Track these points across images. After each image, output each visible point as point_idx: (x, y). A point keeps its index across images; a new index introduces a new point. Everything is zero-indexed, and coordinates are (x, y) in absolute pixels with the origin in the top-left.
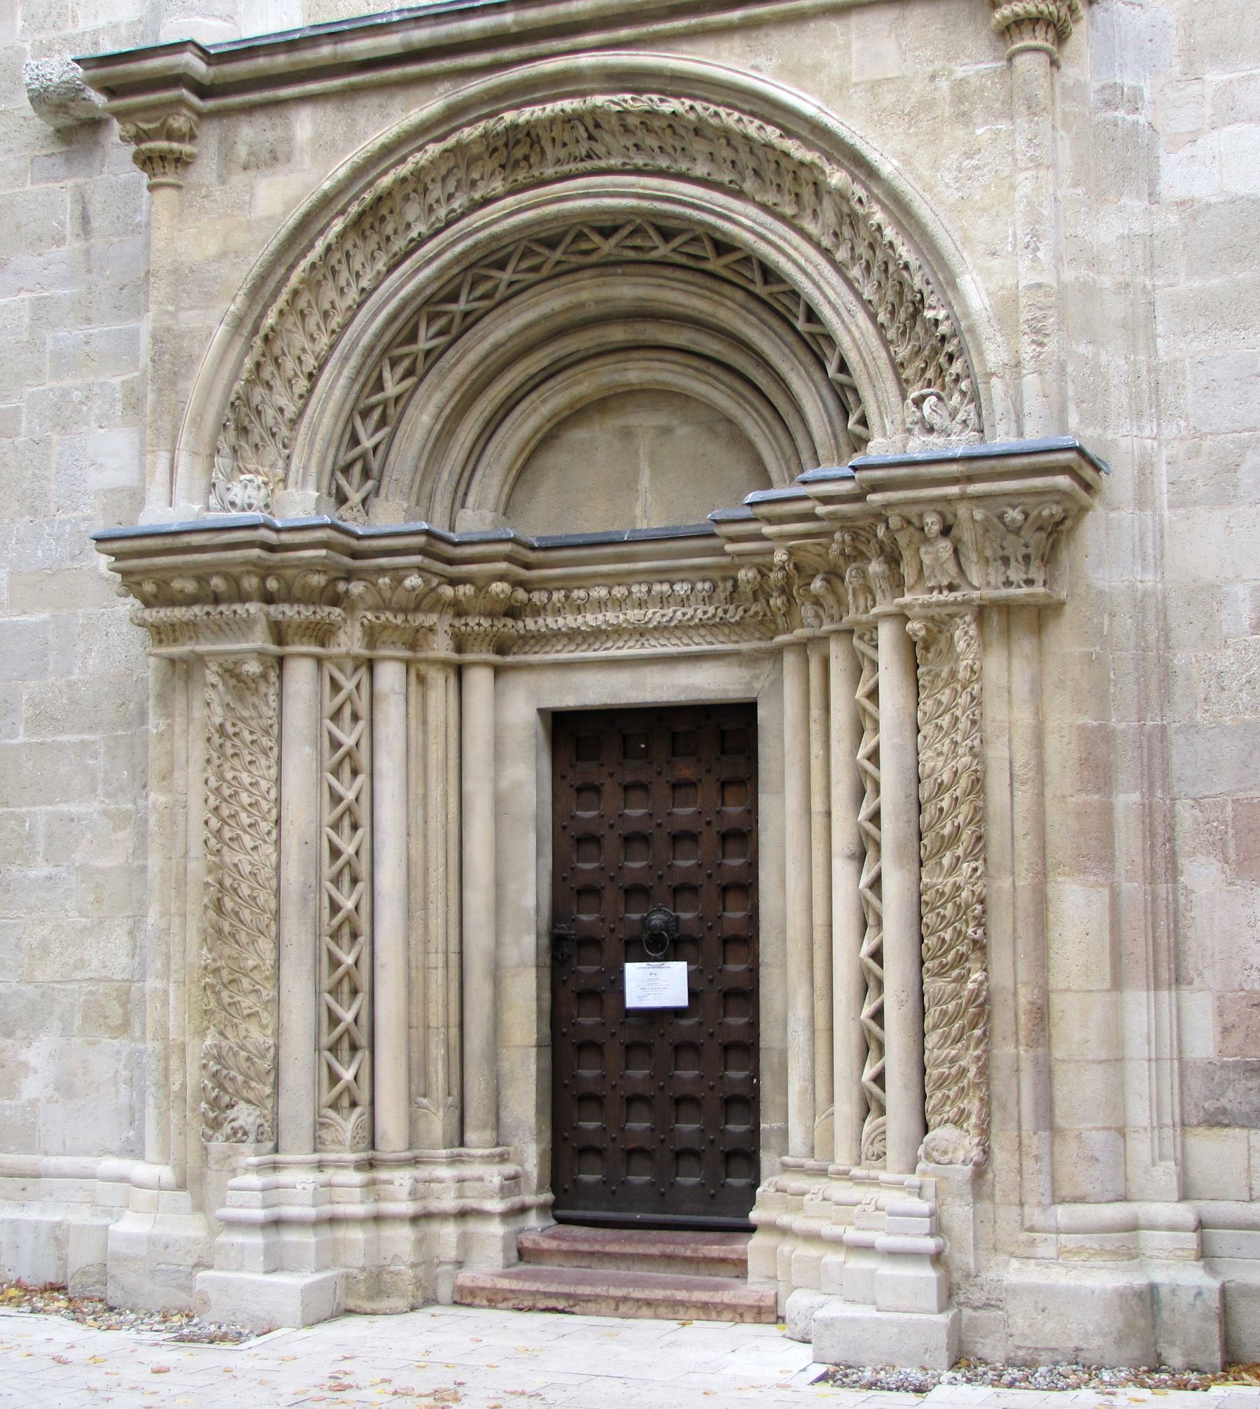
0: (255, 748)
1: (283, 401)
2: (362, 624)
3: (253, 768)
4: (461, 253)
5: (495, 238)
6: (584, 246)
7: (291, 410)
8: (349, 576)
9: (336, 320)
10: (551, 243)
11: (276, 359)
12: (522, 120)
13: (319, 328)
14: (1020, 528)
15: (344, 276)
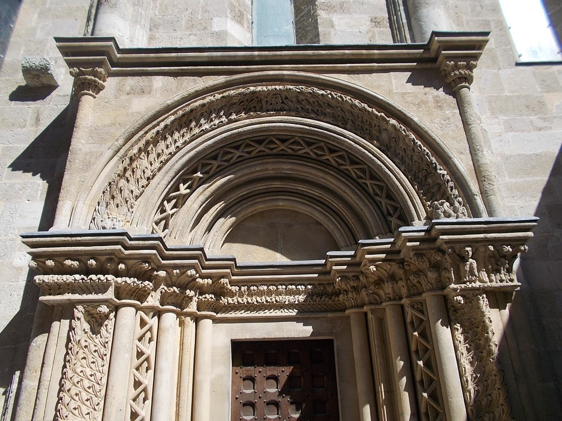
0: (96, 354)
1: (133, 188)
2: (161, 292)
3: (93, 366)
4: (224, 137)
5: (240, 134)
6: (272, 146)
7: (137, 192)
8: (160, 267)
9: (163, 158)
10: (260, 142)
11: (133, 169)
12: (257, 90)
13: (155, 160)
14: (400, 280)
15: (170, 139)
